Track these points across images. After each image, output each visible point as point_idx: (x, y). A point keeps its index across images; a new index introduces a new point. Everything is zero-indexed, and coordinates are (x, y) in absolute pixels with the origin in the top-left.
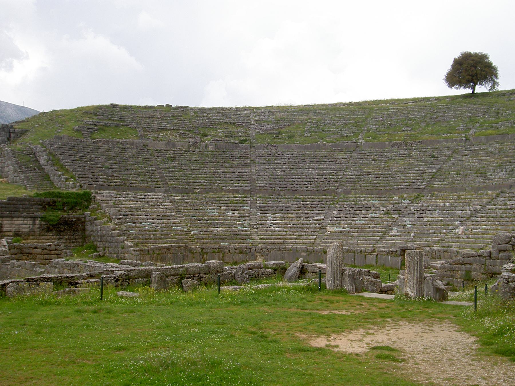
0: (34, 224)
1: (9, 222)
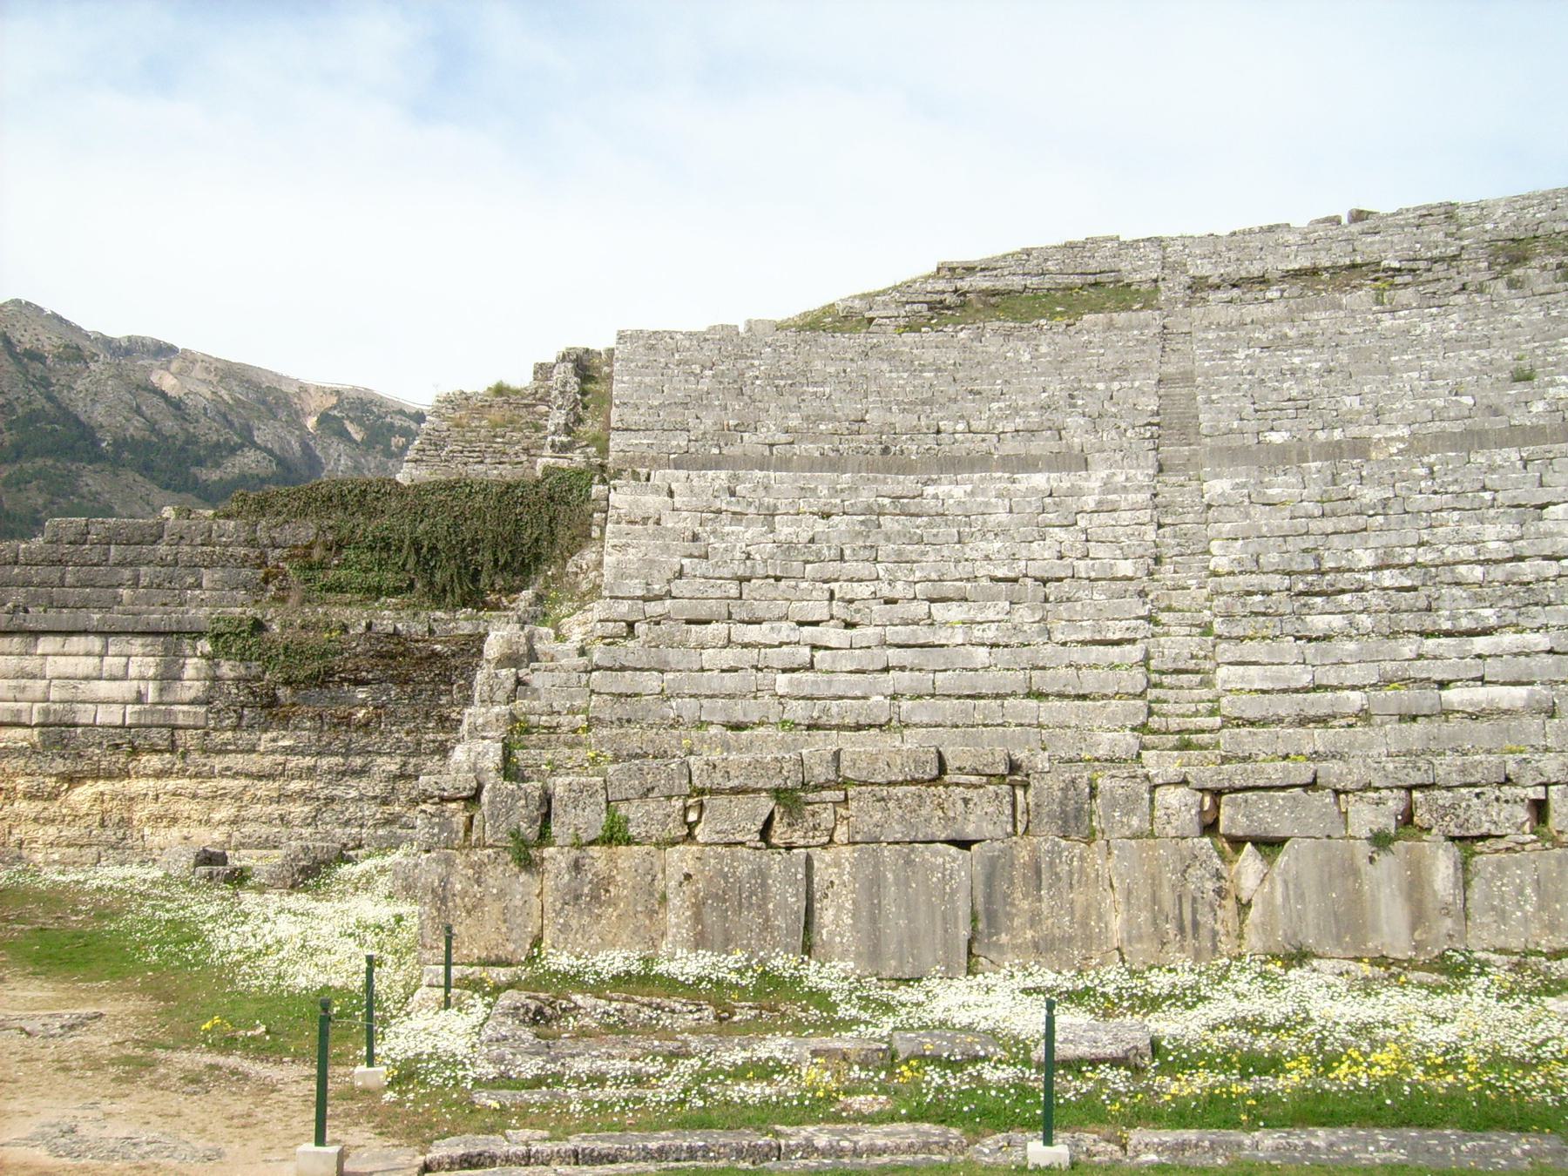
0: (169, 676)
1: (13, 661)
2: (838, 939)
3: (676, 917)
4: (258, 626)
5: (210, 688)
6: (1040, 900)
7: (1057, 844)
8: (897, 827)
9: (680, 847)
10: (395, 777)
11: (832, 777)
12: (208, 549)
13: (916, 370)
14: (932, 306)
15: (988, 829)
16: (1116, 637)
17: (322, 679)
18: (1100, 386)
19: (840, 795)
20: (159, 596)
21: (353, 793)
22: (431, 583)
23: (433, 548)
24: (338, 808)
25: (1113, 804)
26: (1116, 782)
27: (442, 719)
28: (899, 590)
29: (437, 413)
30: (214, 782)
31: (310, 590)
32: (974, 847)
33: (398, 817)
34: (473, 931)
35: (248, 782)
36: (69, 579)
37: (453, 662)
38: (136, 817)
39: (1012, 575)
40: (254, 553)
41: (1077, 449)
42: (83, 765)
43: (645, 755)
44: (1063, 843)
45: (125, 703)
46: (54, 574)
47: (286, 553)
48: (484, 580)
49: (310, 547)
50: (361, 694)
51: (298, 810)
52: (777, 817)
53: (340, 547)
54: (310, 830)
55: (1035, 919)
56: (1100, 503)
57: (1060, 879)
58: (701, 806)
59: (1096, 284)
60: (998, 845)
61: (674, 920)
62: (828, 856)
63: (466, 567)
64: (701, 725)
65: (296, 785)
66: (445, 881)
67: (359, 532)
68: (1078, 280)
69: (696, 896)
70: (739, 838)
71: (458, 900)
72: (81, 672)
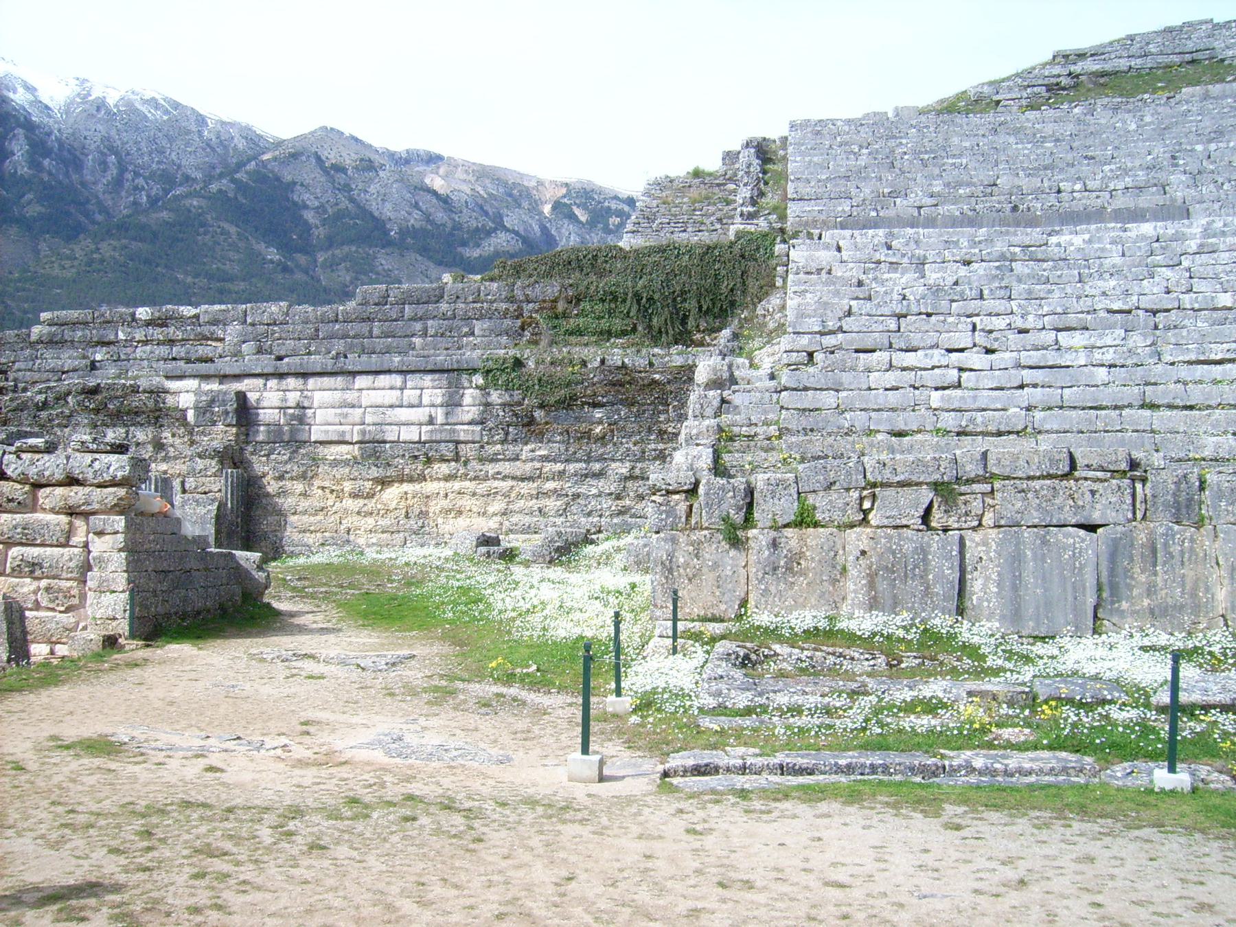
0: (452, 403)
1: (338, 394)
2: (985, 604)
3: (854, 585)
4: (518, 363)
5: (484, 412)
6: (1155, 574)
7: (1171, 529)
8: (1035, 514)
9: (857, 529)
10: (626, 478)
11: (981, 472)
12: (479, 305)
13: (1038, 141)
14: (1049, 88)
15: (1111, 516)
16: (1218, 357)
17: (568, 403)
18: (1199, 148)
19: (988, 487)
20: (443, 342)
21: (594, 491)
22: (650, 327)
23: (650, 299)
24: (582, 502)
25: (1220, 495)
26: (1223, 477)
27: (661, 433)
28: (1031, 322)
29: (647, 193)
30: (489, 483)
31: (556, 334)
32: (1100, 530)
33: (630, 508)
34: (693, 594)
35: (514, 483)
36: (376, 331)
37: (668, 388)
38: (431, 510)
39: (1126, 307)
40: (513, 307)
41: (1180, 201)
42: (391, 472)
43: (826, 457)
44: (1176, 527)
45: (421, 424)
46: (365, 328)
47: (537, 306)
48: (691, 323)
49: (555, 301)
50: (598, 414)
51: (552, 504)
52: (936, 505)
53: (579, 300)
54: (562, 519)
55: (1151, 591)
56: (1201, 245)
57: (1172, 557)
58: (874, 496)
59: (1193, 61)
60: (1119, 528)
61: (852, 587)
62: (977, 537)
63: (677, 314)
64: (870, 432)
65: (550, 485)
66: (671, 556)
67: (593, 288)
68: (1176, 59)
69: (870, 568)
70: (904, 522)
71: (681, 570)
72: (387, 402)
